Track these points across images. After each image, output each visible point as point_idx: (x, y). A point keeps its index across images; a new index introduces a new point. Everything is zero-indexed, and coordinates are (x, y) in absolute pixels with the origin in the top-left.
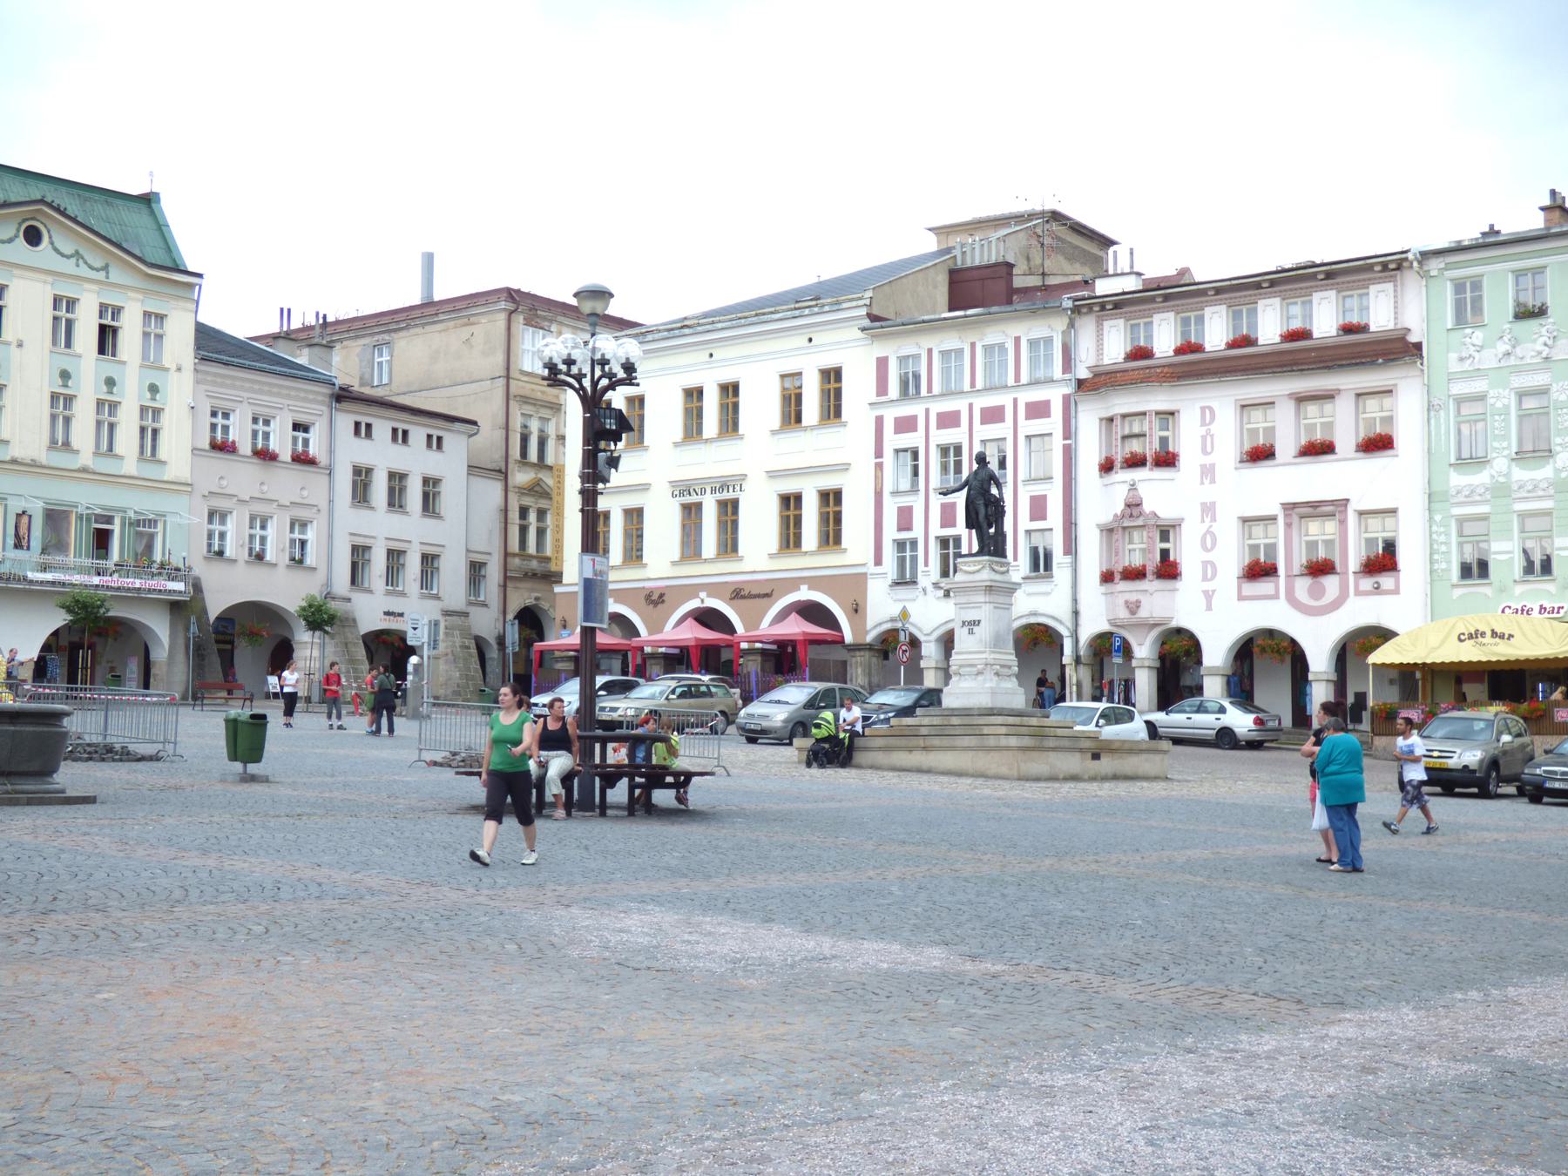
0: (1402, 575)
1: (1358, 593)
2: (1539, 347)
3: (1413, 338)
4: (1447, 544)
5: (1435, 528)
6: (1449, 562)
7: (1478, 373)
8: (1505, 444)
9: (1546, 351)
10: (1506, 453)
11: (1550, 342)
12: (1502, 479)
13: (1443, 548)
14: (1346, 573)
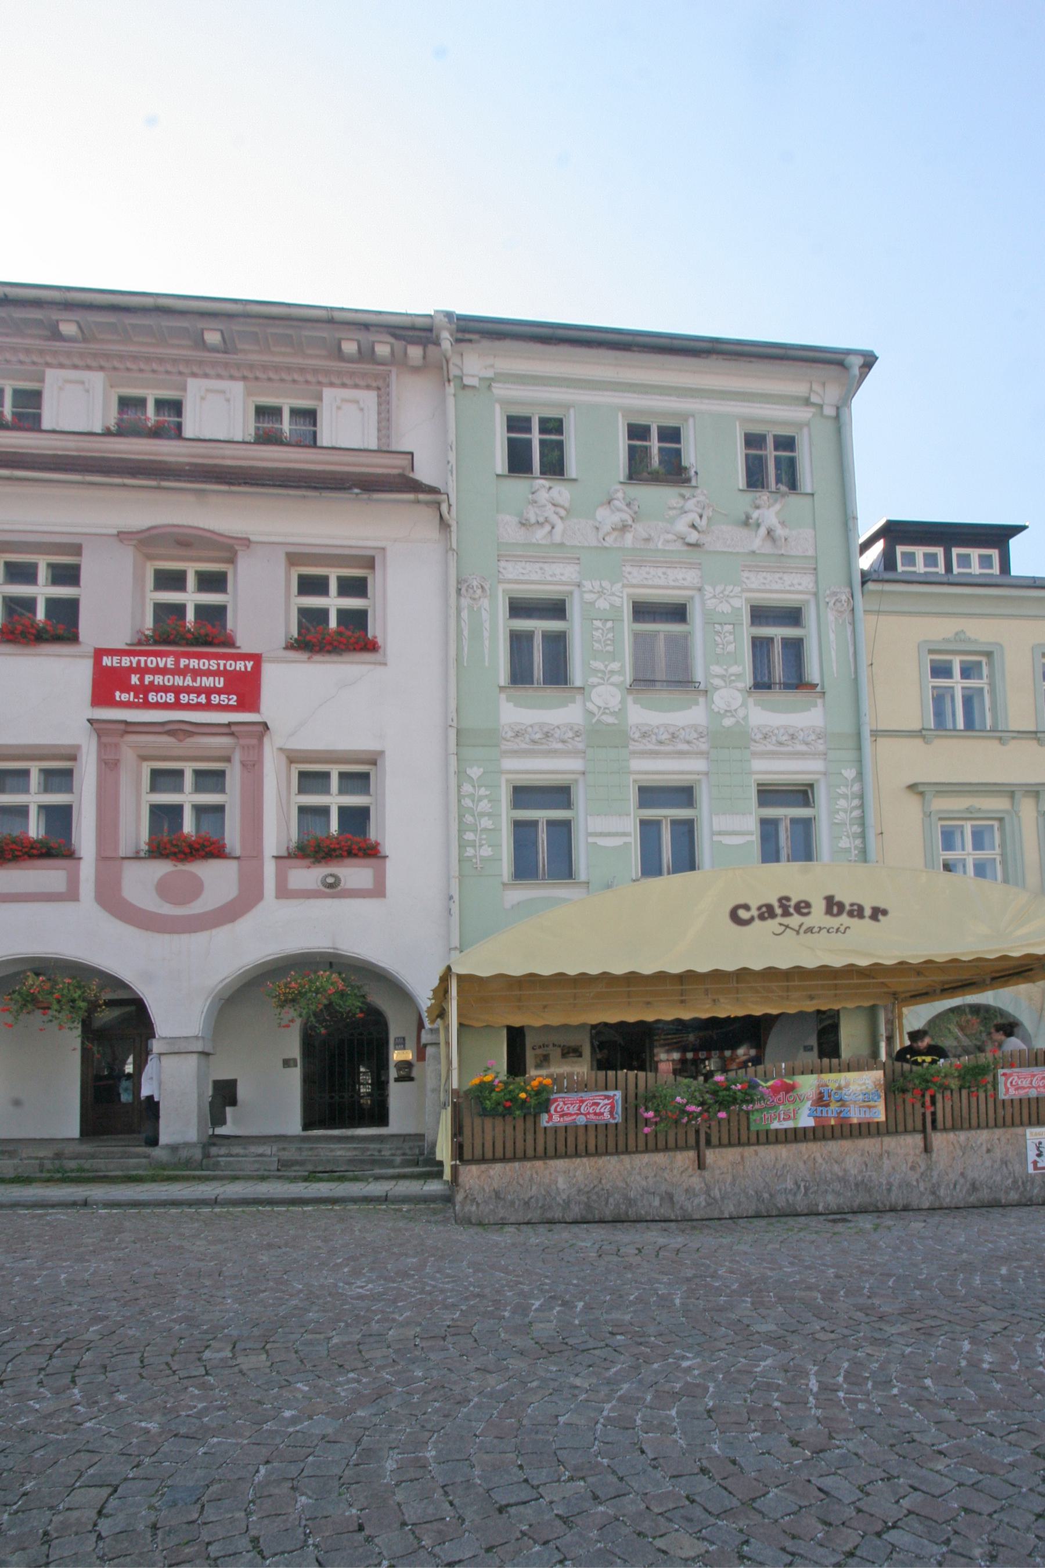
0: (389, 864)
1: (283, 892)
2: (681, 526)
3: (424, 473)
4: (493, 815)
5: (467, 788)
6: (496, 846)
7: (560, 552)
8: (615, 666)
9: (693, 537)
10: (615, 679)
11: (702, 524)
12: (610, 720)
13: (486, 823)
14: (257, 855)
